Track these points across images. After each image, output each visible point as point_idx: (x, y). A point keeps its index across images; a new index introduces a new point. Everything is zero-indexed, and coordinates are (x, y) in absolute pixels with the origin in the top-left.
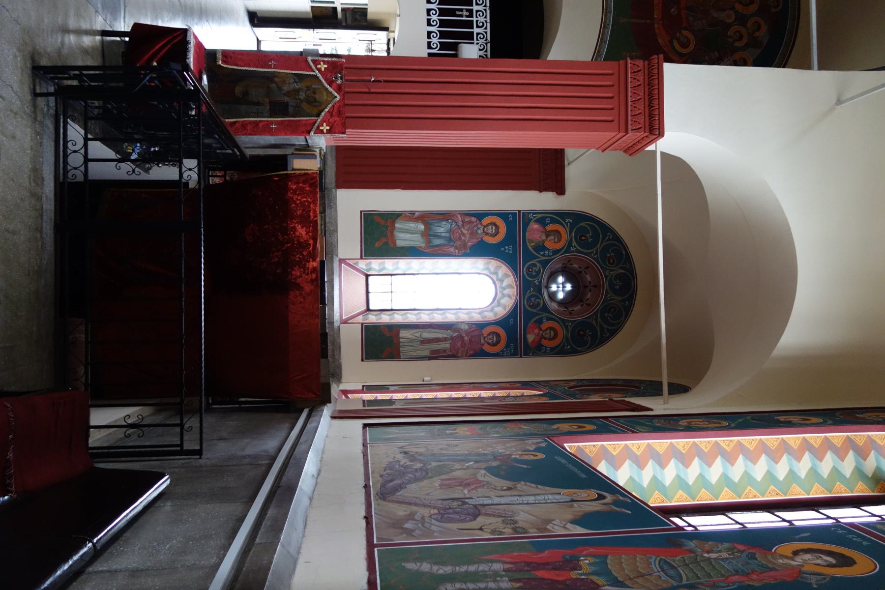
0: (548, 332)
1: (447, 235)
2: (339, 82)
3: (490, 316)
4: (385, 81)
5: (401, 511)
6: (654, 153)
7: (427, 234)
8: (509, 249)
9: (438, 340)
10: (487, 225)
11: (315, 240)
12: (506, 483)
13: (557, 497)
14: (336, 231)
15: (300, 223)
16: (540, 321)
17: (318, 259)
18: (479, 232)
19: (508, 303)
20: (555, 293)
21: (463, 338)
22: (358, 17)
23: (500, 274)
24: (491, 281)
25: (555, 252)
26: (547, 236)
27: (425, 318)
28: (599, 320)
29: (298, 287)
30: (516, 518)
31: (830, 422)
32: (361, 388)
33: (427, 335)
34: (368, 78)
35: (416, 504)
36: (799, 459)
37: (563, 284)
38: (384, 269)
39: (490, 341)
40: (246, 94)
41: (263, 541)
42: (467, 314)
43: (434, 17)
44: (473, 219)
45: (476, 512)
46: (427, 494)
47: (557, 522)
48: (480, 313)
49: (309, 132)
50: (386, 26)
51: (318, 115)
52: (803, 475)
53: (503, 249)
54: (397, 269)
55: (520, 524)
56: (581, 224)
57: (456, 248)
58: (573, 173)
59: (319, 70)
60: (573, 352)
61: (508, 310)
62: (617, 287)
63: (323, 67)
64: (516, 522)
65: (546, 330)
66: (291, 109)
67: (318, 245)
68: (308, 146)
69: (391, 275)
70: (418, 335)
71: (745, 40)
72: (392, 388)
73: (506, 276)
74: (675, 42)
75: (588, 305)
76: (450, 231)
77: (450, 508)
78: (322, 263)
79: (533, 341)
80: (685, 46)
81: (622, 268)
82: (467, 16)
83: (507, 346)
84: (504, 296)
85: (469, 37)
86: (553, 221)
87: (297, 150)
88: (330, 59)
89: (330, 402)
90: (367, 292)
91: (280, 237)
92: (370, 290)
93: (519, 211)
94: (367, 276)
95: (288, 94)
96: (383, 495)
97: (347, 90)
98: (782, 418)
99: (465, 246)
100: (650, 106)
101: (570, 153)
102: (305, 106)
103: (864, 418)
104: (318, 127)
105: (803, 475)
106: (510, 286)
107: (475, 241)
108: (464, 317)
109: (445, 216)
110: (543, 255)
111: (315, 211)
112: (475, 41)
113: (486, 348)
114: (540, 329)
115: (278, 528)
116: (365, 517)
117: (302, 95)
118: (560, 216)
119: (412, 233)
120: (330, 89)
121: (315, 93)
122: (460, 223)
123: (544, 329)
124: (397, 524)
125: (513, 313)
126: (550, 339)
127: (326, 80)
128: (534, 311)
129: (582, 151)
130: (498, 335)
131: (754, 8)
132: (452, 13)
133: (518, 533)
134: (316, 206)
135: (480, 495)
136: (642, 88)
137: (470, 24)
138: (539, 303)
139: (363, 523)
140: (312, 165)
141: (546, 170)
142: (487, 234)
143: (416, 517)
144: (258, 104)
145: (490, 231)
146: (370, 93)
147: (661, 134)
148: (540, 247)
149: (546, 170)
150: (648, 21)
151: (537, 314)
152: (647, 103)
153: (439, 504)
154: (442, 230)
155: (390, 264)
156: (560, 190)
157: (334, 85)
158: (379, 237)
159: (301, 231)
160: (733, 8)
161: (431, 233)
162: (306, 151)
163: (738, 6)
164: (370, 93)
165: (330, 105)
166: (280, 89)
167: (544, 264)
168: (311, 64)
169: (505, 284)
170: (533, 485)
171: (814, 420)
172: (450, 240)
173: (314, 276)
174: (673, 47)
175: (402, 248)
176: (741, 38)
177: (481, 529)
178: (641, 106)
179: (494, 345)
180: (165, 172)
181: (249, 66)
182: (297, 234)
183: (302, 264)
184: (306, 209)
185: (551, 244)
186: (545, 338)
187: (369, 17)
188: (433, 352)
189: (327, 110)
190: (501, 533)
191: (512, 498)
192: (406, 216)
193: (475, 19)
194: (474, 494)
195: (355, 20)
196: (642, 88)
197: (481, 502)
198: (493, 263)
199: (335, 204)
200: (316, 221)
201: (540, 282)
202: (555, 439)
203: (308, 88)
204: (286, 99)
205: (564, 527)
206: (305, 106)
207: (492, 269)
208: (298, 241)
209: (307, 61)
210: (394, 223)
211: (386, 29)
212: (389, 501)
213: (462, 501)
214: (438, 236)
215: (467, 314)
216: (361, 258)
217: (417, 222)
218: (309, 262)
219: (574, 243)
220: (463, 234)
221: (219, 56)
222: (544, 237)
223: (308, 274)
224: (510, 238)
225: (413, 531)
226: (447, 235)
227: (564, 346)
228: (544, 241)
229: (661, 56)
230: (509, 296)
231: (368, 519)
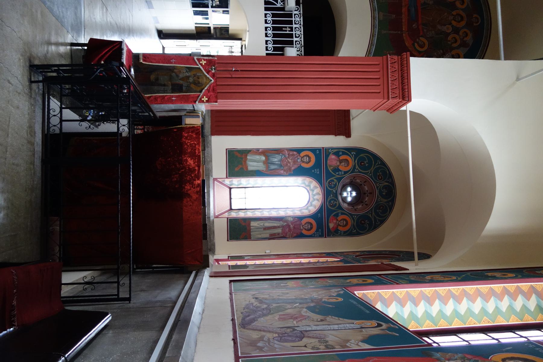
0: (342, 221)
1: (279, 163)
2: (213, 71)
3: (306, 212)
4: (241, 71)
5: (255, 335)
6: (405, 111)
7: (267, 163)
8: (317, 171)
9: (275, 227)
10: (304, 157)
11: (199, 167)
12: (320, 317)
13: (352, 325)
15: (189, 157)
16: (337, 215)
17: (201, 179)
18: (299, 160)
19: (317, 204)
20: (346, 198)
21: (288, 226)
22: (223, 32)
23: (312, 187)
24: (306, 191)
25: (345, 173)
26: (340, 163)
27: (266, 214)
28: (373, 213)
29: (189, 196)
30: (327, 339)
31: (520, 276)
32: (227, 258)
33: (267, 224)
34: (230, 69)
35: (264, 331)
36: (501, 300)
37: (350, 192)
38: (241, 184)
39: (307, 228)
40: (157, 79)
41: (171, 355)
42: (292, 211)
43: (270, 32)
44: (295, 153)
45: (302, 335)
46: (271, 325)
47: (353, 341)
48: (300, 211)
49: (195, 102)
50: (240, 37)
51: (201, 92)
52: (504, 309)
54: (249, 184)
55: (330, 343)
57: (284, 171)
58: (354, 124)
59: (201, 64)
60: (358, 234)
61: (317, 208)
62: (384, 194)
63: (204, 62)
64: (327, 342)
65: (341, 220)
66: (184, 88)
67: (201, 170)
68: (194, 110)
69: (245, 188)
70: (262, 224)
71: (459, 42)
72: (246, 258)
73: (316, 187)
74: (416, 44)
75: (367, 205)
76: (281, 160)
77: (286, 333)
78: (203, 181)
79: (333, 228)
80: (422, 47)
81: (386, 182)
82: (289, 31)
83: (317, 231)
84: (314, 200)
85: (291, 43)
86: (344, 153)
87: (187, 112)
88: (207, 58)
89: (208, 267)
90: (231, 199)
91: (178, 166)
92: (232, 197)
93: (323, 148)
94: (230, 189)
95: (182, 79)
96: (244, 325)
97: (218, 76)
98: (489, 274)
99: (290, 169)
100: (403, 83)
101: (353, 113)
102: (193, 86)
103: (541, 274)
104: (201, 99)
105: (504, 309)
106: (318, 194)
107: (296, 166)
108: (290, 213)
109: (278, 151)
110: (338, 174)
111: (199, 149)
112: (295, 46)
113: (304, 232)
114: (337, 220)
115: (179, 347)
116: (233, 339)
117: (191, 80)
118: (348, 150)
119: (258, 162)
120: (208, 76)
121: (199, 78)
122: (287, 156)
123: (339, 220)
124: (253, 344)
126: (343, 226)
127: (205, 70)
128: (333, 209)
129: (362, 110)
130: (311, 224)
131: (463, 23)
132: (280, 29)
133: (329, 348)
134: (199, 146)
135: (304, 324)
136: (397, 72)
137: (291, 36)
138: (336, 204)
139: (232, 342)
140: (197, 122)
141: (339, 123)
142: (303, 162)
143: (264, 339)
144: (164, 85)
145: (305, 160)
146: (232, 78)
147: (409, 100)
148: (336, 170)
149: (339, 123)
150: (399, 32)
151: (335, 211)
152: (400, 81)
153: (279, 330)
154: (276, 160)
155: (244, 181)
156: (348, 134)
157: (210, 73)
158: (237, 164)
159: (191, 162)
160: (450, 24)
162: (193, 113)
163: (454, 23)
164: (232, 78)
165: (208, 86)
166: (178, 76)
167: (339, 180)
168: (197, 61)
169: (315, 193)
170: (336, 318)
171: (510, 275)
172: (281, 166)
173: (198, 189)
174: (415, 48)
175: (252, 171)
176: (456, 41)
177: (305, 346)
178: (396, 83)
179: (309, 230)
180: (108, 127)
181: (159, 63)
182: (188, 163)
183: (191, 182)
184: (194, 148)
185: (343, 168)
186: (340, 226)
187: (230, 32)
188: (271, 235)
189: (206, 88)
190: (318, 349)
191: (324, 326)
192: (254, 152)
193: (294, 33)
194: (300, 324)
195: (221, 34)
196: (397, 72)
197: (305, 329)
198: (307, 180)
199: (211, 145)
200: (200, 155)
201: (337, 191)
202: (349, 289)
203: (195, 75)
204: (181, 82)
205: (357, 345)
206: (193, 86)
207: (307, 183)
208: (189, 167)
209: (194, 59)
210: (246, 156)
211: (240, 39)
212: (247, 329)
213: (293, 328)
214: (273, 164)
215: (292, 211)
216: (227, 178)
218: (195, 180)
219: (357, 167)
220: (289, 162)
221: (141, 57)
222: (338, 164)
223: (194, 188)
224: (318, 165)
225: (263, 348)
226: (279, 163)
227: (352, 230)
228: (338, 166)
229: (408, 53)
230: (318, 200)
231: (235, 340)
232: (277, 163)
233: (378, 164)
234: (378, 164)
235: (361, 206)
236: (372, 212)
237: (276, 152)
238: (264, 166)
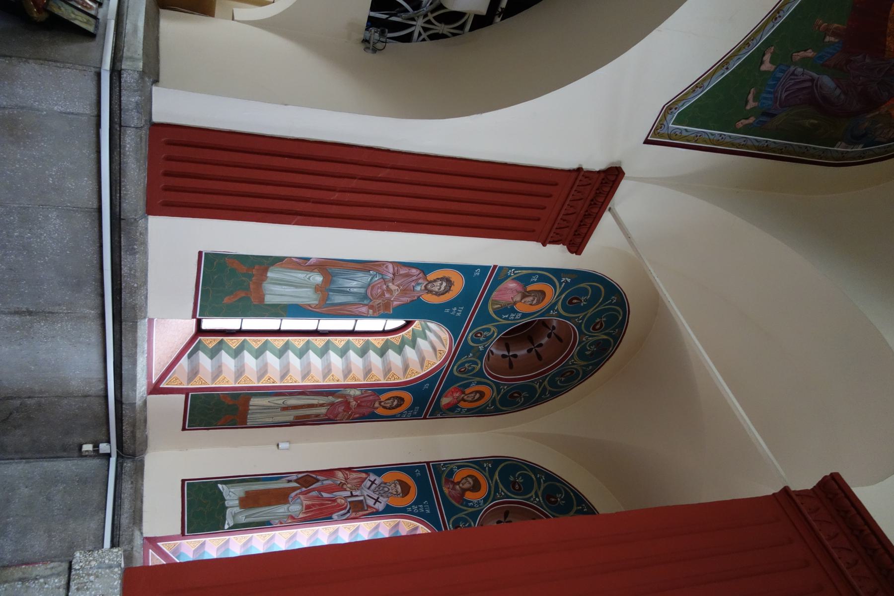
1: (362, 291)
10: (435, 281)
14: (145, 283)
16: (467, 385)
21: (347, 403)
26: (524, 296)
33: (293, 401)
44: (414, 271)
53: (447, 310)
56: (582, 285)
57: (371, 307)
60: (497, 412)
70: (280, 402)
79: (448, 404)
81: (605, 334)
86: (543, 279)
99: (387, 305)
107: (406, 299)
110: (505, 319)
113: (380, 411)
119: (296, 287)
125: (432, 378)
130: (401, 400)
142: (430, 292)
154: (354, 284)
156: (576, 248)
161: (333, 287)
172: (365, 297)
186: (465, 401)
188: (297, 417)
199: (145, 243)
210: (266, 270)
217: (312, 271)
220: (389, 290)
222: (518, 298)
224: (465, 299)
228: (515, 303)
232: (355, 290)
233: (610, 304)
234: (610, 304)
235: (524, 352)
236: (544, 381)
237: (359, 266)
238: (314, 296)
